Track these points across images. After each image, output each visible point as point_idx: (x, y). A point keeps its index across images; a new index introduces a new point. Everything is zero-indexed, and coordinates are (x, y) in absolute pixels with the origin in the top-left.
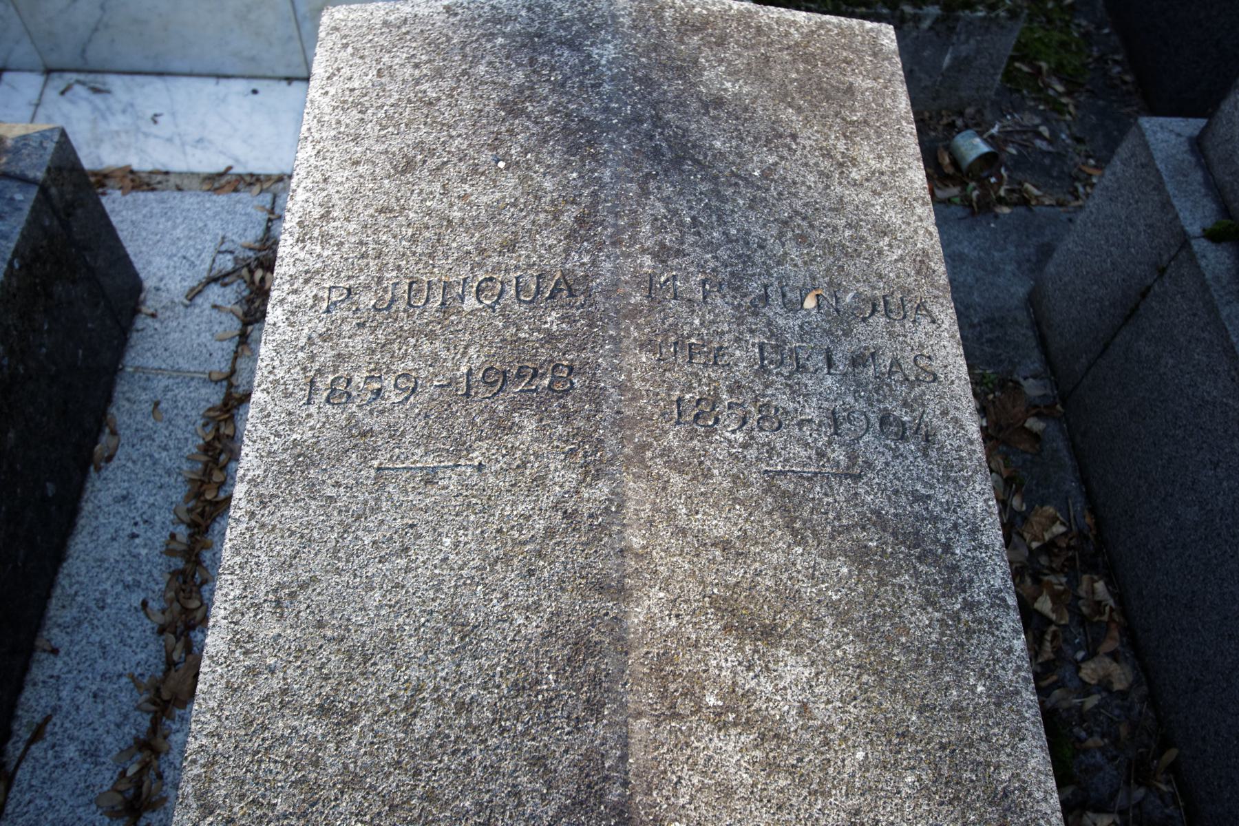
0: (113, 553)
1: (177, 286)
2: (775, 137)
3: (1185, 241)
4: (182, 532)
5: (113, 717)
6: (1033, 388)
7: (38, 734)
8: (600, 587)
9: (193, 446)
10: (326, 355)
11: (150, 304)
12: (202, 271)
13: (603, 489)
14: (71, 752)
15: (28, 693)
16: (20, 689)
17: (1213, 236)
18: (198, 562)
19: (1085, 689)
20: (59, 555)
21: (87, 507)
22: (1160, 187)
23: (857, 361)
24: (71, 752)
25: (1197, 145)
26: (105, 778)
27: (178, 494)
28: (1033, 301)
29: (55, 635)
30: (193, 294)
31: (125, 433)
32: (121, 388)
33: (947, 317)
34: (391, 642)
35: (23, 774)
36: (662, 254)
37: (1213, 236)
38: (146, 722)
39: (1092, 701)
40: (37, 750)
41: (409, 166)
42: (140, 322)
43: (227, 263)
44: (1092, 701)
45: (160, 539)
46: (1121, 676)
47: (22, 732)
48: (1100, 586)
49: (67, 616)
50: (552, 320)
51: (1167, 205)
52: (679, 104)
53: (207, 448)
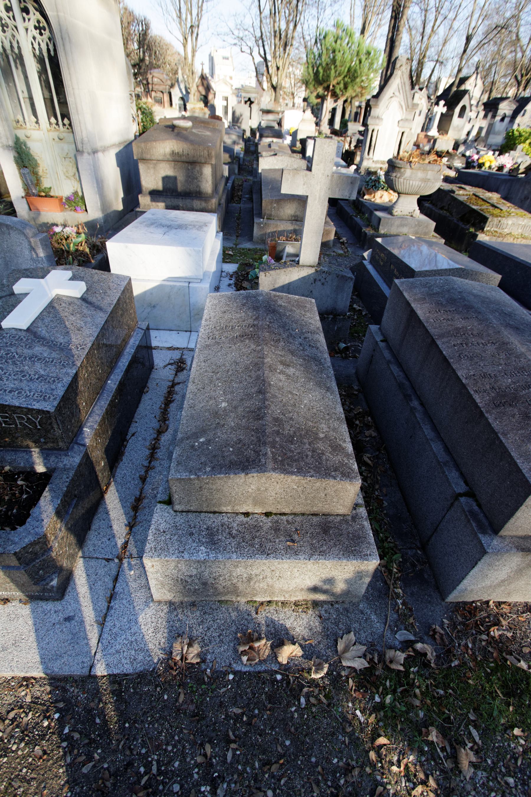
0: (148, 408)
1: (161, 365)
2: (291, 310)
3: (377, 342)
4: (163, 406)
5: (149, 434)
6: (356, 388)
7: (133, 435)
8: (260, 358)
9: (165, 391)
10: (211, 334)
11: (155, 368)
12: (167, 362)
13: (260, 347)
14: (140, 439)
15: (131, 428)
16: (129, 427)
17: (382, 341)
18: (167, 410)
19: (367, 437)
20: (137, 407)
21: (143, 400)
22: (373, 336)
23: (305, 338)
24: (140, 439)
25: (380, 329)
26: (148, 444)
27: (162, 399)
28: (356, 373)
29: (136, 419)
30: (165, 366)
31: (150, 388)
32: (149, 381)
33: (322, 335)
34: (224, 365)
35: (130, 441)
36: (270, 322)
37: (382, 341)
38: (156, 436)
39: (368, 439)
40: (133, 438)
41: (225, 312)
42: (153, 370)
43: (173, 361)
44: (368, 439)
45: (158, 406)
46: (374, 434)
47: (130, 434)
48: (369, 418)
49: (139, 417)
50: (251, 329)
51: (374, 337)
52: (274, 305)
53: (168, 392)
